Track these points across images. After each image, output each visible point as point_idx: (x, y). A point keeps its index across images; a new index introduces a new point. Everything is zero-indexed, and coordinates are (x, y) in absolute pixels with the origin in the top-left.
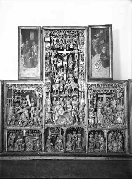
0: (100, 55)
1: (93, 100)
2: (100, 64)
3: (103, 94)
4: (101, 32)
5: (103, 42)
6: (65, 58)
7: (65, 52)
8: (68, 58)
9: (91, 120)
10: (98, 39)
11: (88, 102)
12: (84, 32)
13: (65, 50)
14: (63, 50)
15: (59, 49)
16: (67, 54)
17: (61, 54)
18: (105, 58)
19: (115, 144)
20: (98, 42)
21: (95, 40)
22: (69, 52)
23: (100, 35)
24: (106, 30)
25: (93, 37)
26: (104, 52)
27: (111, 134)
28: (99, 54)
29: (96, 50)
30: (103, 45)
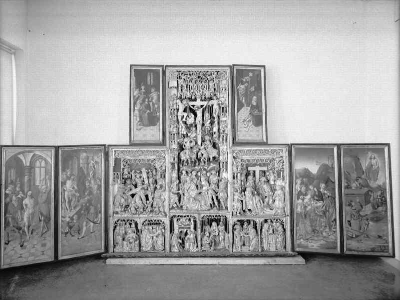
0: (249, 108)
1: (241, 174)
2: (249, 121)
3: (254, 165)
4: (251, 74)
5: (253, 90)
6: (199, 113)
7: (198, 103)
8: (203, 112)
9: (238, 205)
10: (246, 85)
11: (234, 178)
12: (226, 73)
13: (199, 100)
14: (195, 100)
15: (191, 99)
16: (202, 106)
17: (194, 106)
18: (256, 112)
19: (272, 239)
20: (247, 89)
21: (242, 87)
22: (205, 103)
23: (250, 79)
24: (256, 73)
25: (240, 82)
26: (254, 104)
27: (266, 226)
28: (248, 106)
29: (244, 101)
30: (253, 93)
